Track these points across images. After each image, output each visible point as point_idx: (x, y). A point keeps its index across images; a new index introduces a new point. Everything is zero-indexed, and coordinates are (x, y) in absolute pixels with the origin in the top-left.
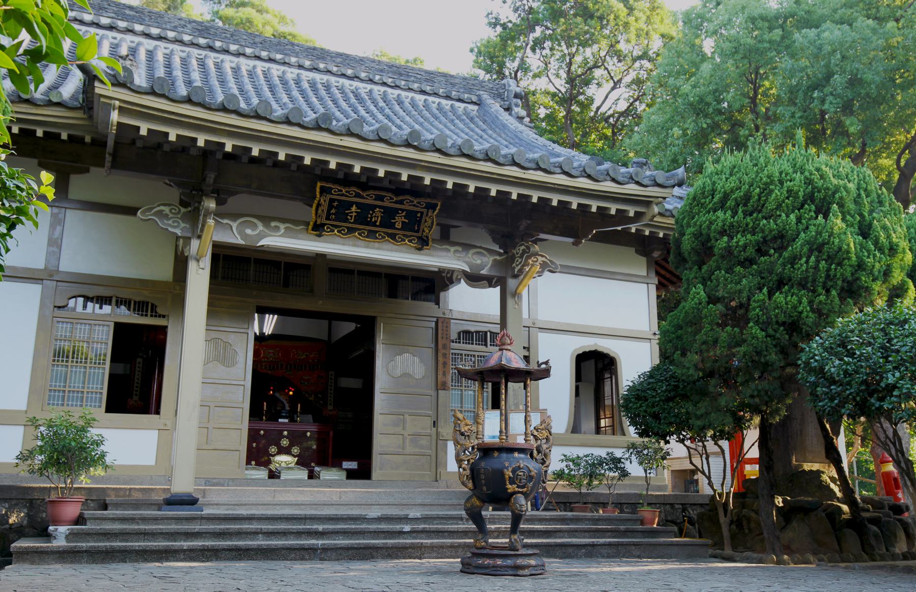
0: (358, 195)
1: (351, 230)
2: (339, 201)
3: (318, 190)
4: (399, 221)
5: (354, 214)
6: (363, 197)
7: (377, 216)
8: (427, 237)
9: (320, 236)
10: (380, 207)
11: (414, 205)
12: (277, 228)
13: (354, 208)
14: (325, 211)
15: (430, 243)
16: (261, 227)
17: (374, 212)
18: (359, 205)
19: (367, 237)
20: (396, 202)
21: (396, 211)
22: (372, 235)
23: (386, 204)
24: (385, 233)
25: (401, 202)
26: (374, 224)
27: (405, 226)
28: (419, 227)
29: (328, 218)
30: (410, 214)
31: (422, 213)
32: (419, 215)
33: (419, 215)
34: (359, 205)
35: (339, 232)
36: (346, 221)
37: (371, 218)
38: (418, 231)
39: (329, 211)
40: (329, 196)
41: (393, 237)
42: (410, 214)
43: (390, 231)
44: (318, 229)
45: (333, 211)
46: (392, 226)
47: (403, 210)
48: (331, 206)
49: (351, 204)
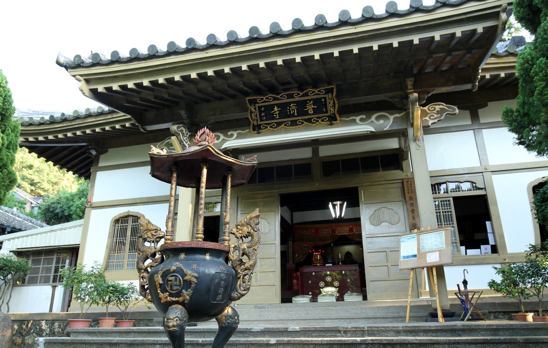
0: (275, 99)
1: (279, 124)
2: (264, 106)
3: (247, 102)
4: (310, 108)
5: (277, 112)
6: (278, 99)
7: (293, 109)
8: (334, 114)
9: (259, 133)
10: (293, 102)
11: (317, 94)
12: (232, 135)
13: (276, 109)
14: (258, 116)
15: (338, 118)
16: (222, 137)
17: (290, 107)
18: (278, 105)
19: (290, 126)
20: (302, 96)
21: (305, 103)
22: (294, 123)
23: (297, 99)
24: (303, 120)
25: (306, 95)
26: (293, 115)
27: (316, 111)
28: (326, 108)
29: (261, 120)
30: (316, 102)
31: (325, 98)
32: (323, 100)
33: (323, 100)
34: (278, 105)
35: (271, 127)
36: (274, 118)
37: (290, 112)
38: (326, 112)
39: (260, 115)
40: (257, 105)
41: (309, 121)
42: (316, 102)
43: (306, 117)
44: (258, 129)
45: (263, 114)
46: (307, 113)
47: (310, 100)
48: (260, 112)
49: (273, 106)
